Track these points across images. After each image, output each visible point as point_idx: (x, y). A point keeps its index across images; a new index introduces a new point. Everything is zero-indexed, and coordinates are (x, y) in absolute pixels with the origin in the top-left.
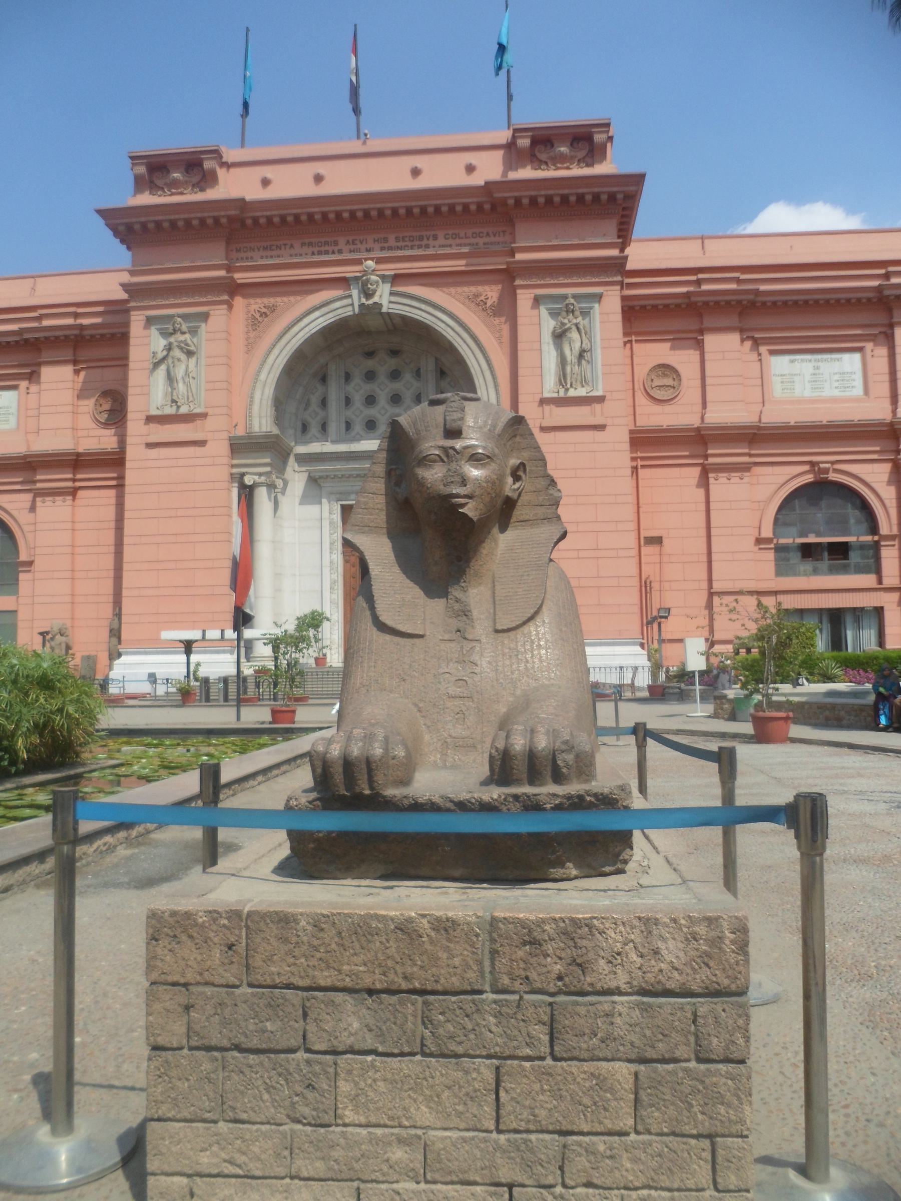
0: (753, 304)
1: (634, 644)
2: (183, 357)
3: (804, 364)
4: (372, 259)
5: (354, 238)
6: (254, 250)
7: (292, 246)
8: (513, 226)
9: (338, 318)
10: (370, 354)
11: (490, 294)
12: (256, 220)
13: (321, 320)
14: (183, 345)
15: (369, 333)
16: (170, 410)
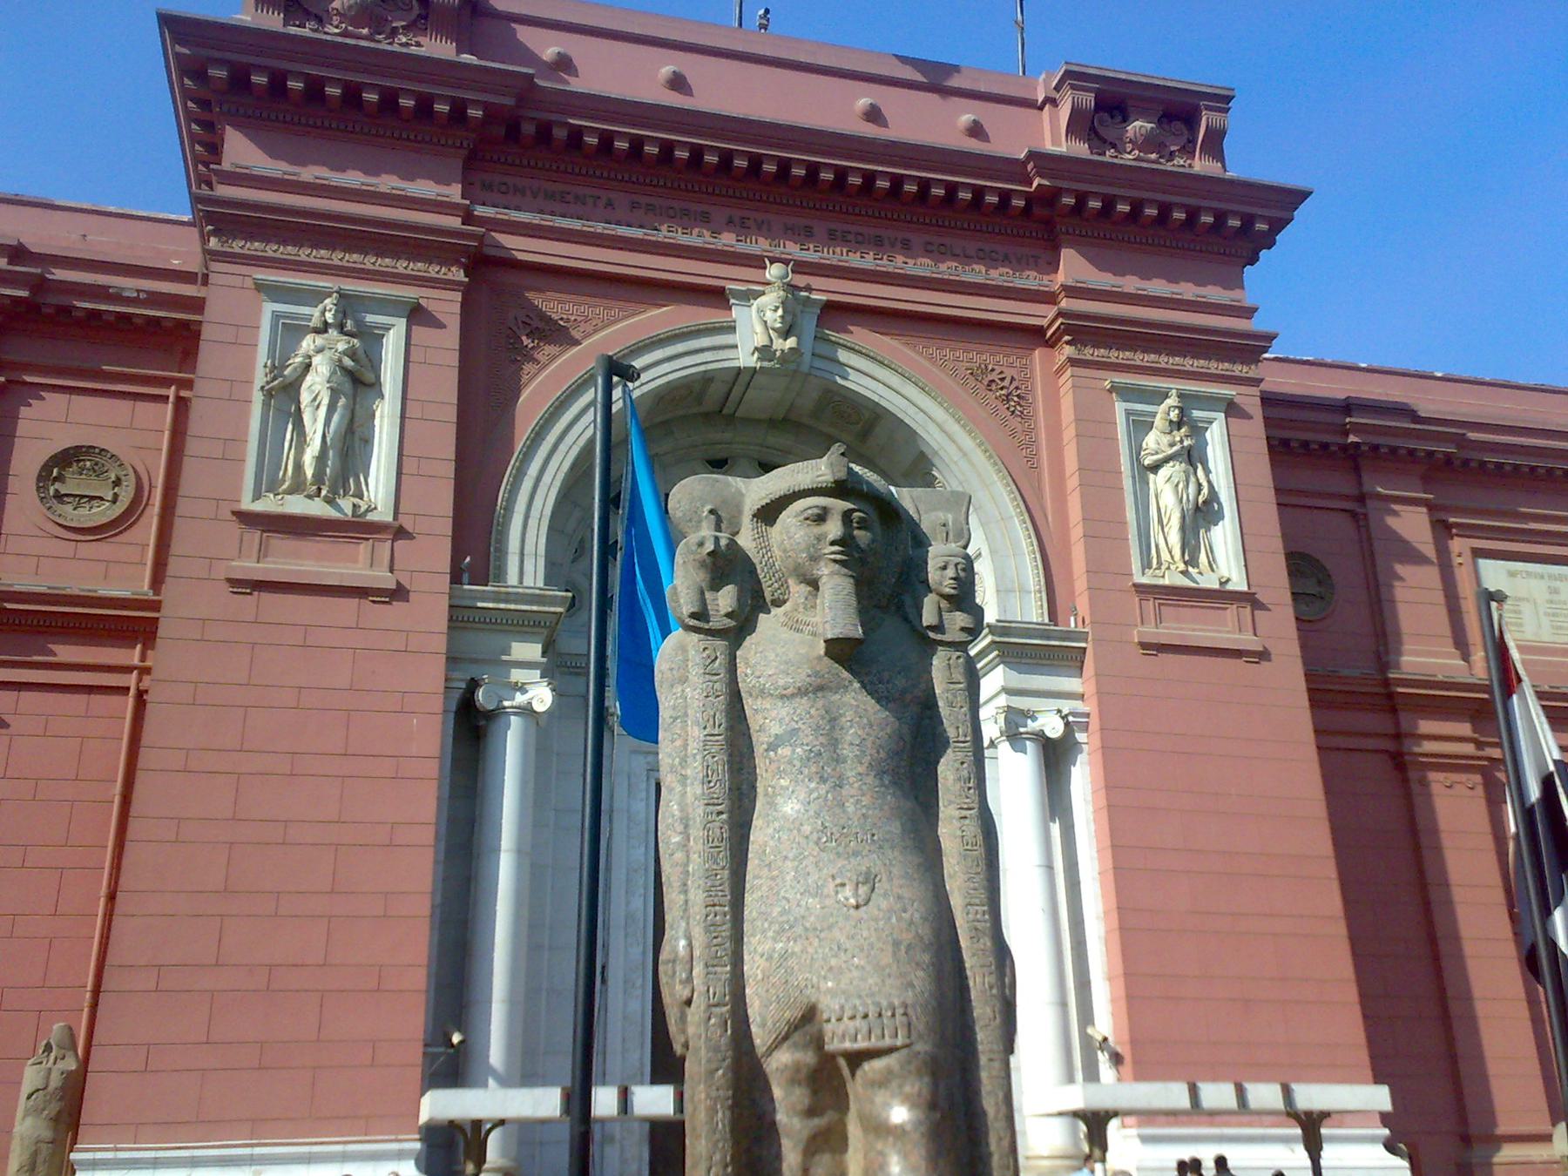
0: (1449, 459)
1: (1372, 1140)
2: (348, 386)
3: (1534, 582)
4: (786, 262)
5: (746, 214)
6: (524, 195)
7: (610, 204)
8: (1056, 249)
9: (702, 368)
10: (719, 464)
11: (1008, 373)
12: (545, 131)
13: (666, 367)
14: (348, 362)
15: (731, 419)
16: (297, 505)
